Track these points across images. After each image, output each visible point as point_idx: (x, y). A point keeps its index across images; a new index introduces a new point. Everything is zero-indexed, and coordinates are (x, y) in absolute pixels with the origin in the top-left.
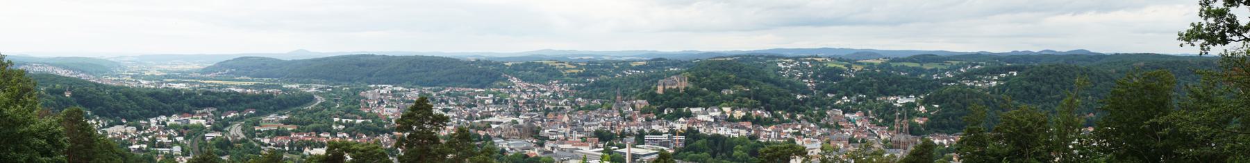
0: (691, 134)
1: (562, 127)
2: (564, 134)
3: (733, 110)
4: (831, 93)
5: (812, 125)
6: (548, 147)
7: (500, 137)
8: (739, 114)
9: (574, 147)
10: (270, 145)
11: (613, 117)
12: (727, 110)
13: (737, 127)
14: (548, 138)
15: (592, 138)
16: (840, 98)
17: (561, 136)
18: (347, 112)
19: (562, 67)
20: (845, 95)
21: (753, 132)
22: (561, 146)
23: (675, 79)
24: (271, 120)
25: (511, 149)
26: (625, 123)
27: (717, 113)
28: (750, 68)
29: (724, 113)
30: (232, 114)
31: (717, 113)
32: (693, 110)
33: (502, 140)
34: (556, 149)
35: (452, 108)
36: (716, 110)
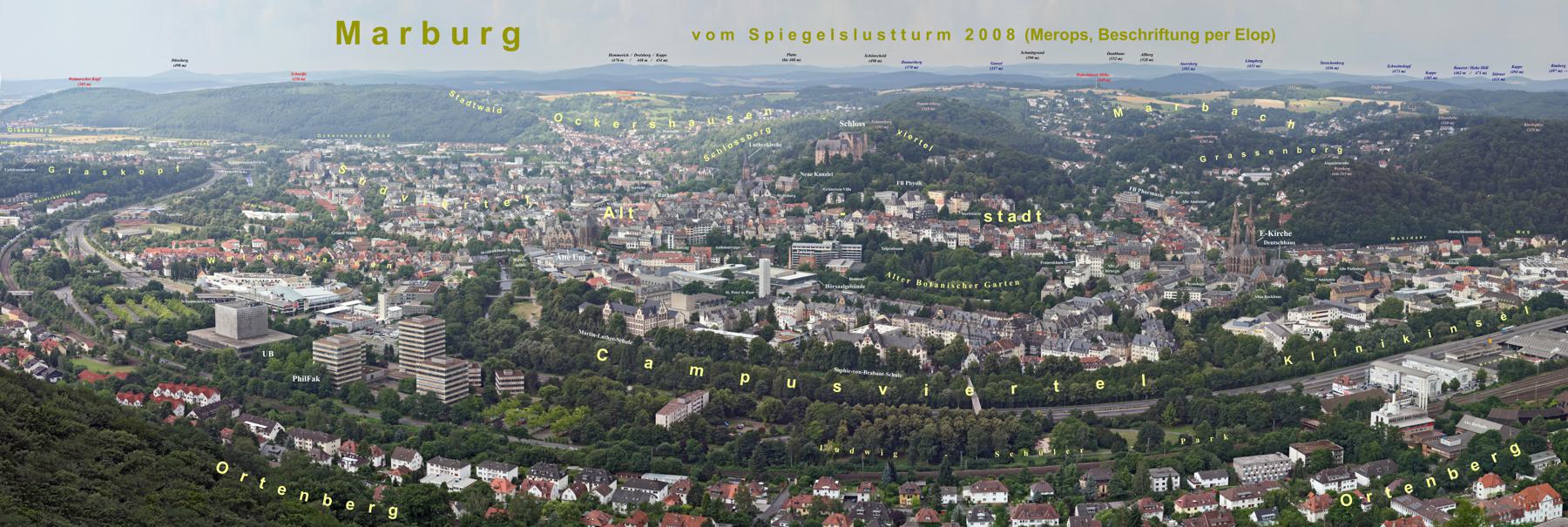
0: (872, 242)
1: (648, 227)
2: (652, 240)
3: (947, 198)
4: (1124, 161)
5: (1087, 225)
6: (623, 264)
7: (539, 244)
8: (958, 205)
9: (670, 265)
10: (135, 264)
11: (737, 209)
12: (938, 197)
13: (953, 230)
14: (623, 247)
15: (701, 249)
16: (1137, 170)
17: (647, 244)
18: (272, 197)
19: (645, 104)
20: (1148, 166)
21: (982, 238)
22: (645, 263)
23: (847, 137)
24: (134, 219)
25: (560, 270)
26: (757, 221)
27: (919, 203)
28: (979, 112)
29: (932, 202)
30: (66, 205)
31: (919, 203)
32: (878, 195)
33: (543, 252)
34: (637, 270)
35: (450, 185)
36: (917, 197)
